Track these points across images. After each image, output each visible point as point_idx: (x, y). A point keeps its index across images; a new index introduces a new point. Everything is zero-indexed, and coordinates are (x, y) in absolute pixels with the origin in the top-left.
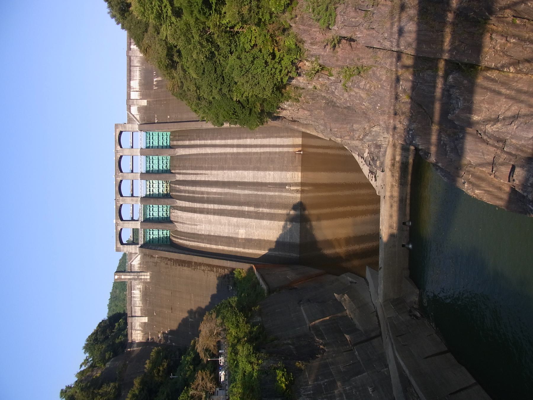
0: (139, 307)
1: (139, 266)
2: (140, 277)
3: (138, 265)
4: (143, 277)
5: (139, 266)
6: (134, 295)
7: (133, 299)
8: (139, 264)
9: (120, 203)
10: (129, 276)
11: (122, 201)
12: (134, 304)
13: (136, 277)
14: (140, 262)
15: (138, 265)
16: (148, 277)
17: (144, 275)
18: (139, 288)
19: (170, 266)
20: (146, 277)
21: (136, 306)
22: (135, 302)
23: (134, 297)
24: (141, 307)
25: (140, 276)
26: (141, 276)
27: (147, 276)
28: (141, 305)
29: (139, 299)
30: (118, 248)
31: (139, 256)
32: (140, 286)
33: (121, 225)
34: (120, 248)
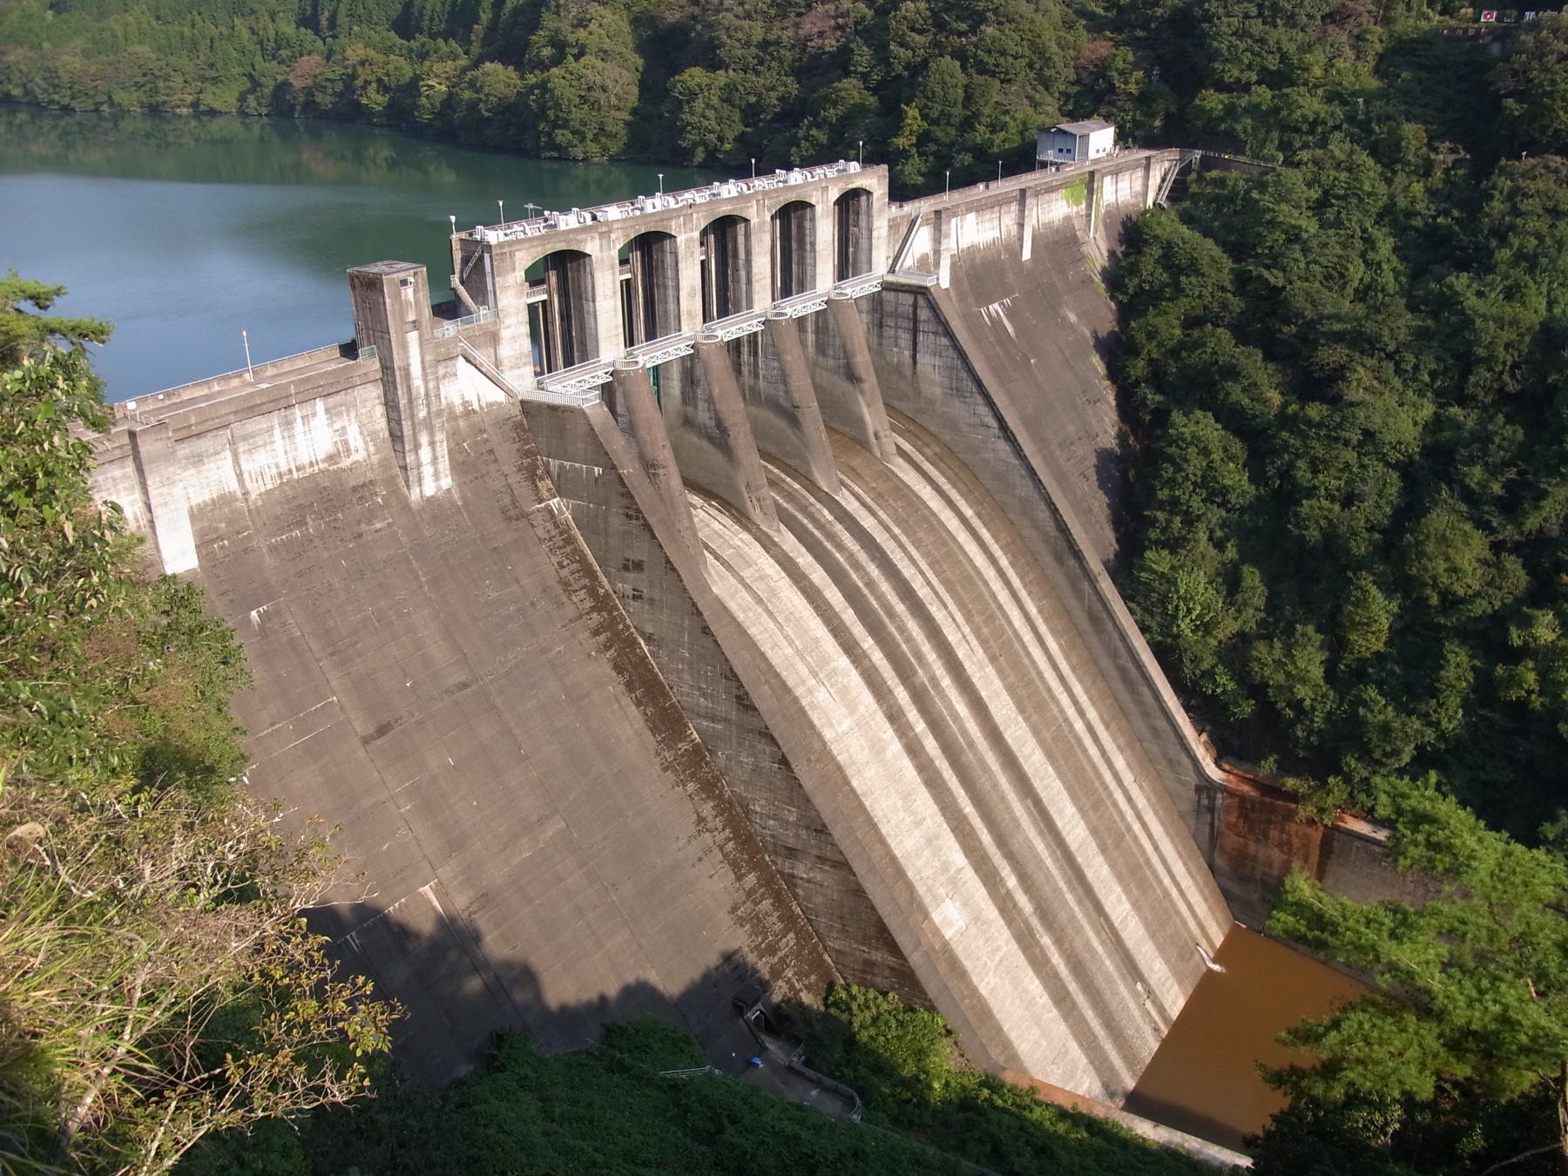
0: (240, 476)
1: (459, 410)
2: (424, 439)
3: (457, 402)
4: (425, 454)
5: (459, 410)
6: (299, 421)
7: (275, 419)
8: (465, 403)
9: (680, 232)
10: (423, 362)
11: (687, 240)
12: (245, 438)
13: (422, 414)
14: (476, 407)
15: (457, 402)
16: (429, 489)
17: (435, 460)
18: (346, 442)
19: (570, 611)
20: (427, 471)
21: (235, 455)
22: (259, 440)
23: (288, 424)
24: (246, 493)
25: (432, 434)
26: (432, 444)
27: (436, 476)
28: (256, 490)
29: (284, 468)
30: (512, 254)
31: (498, 396)
32: (360, 444)
33: (605, 254)
34: (514, 270)
